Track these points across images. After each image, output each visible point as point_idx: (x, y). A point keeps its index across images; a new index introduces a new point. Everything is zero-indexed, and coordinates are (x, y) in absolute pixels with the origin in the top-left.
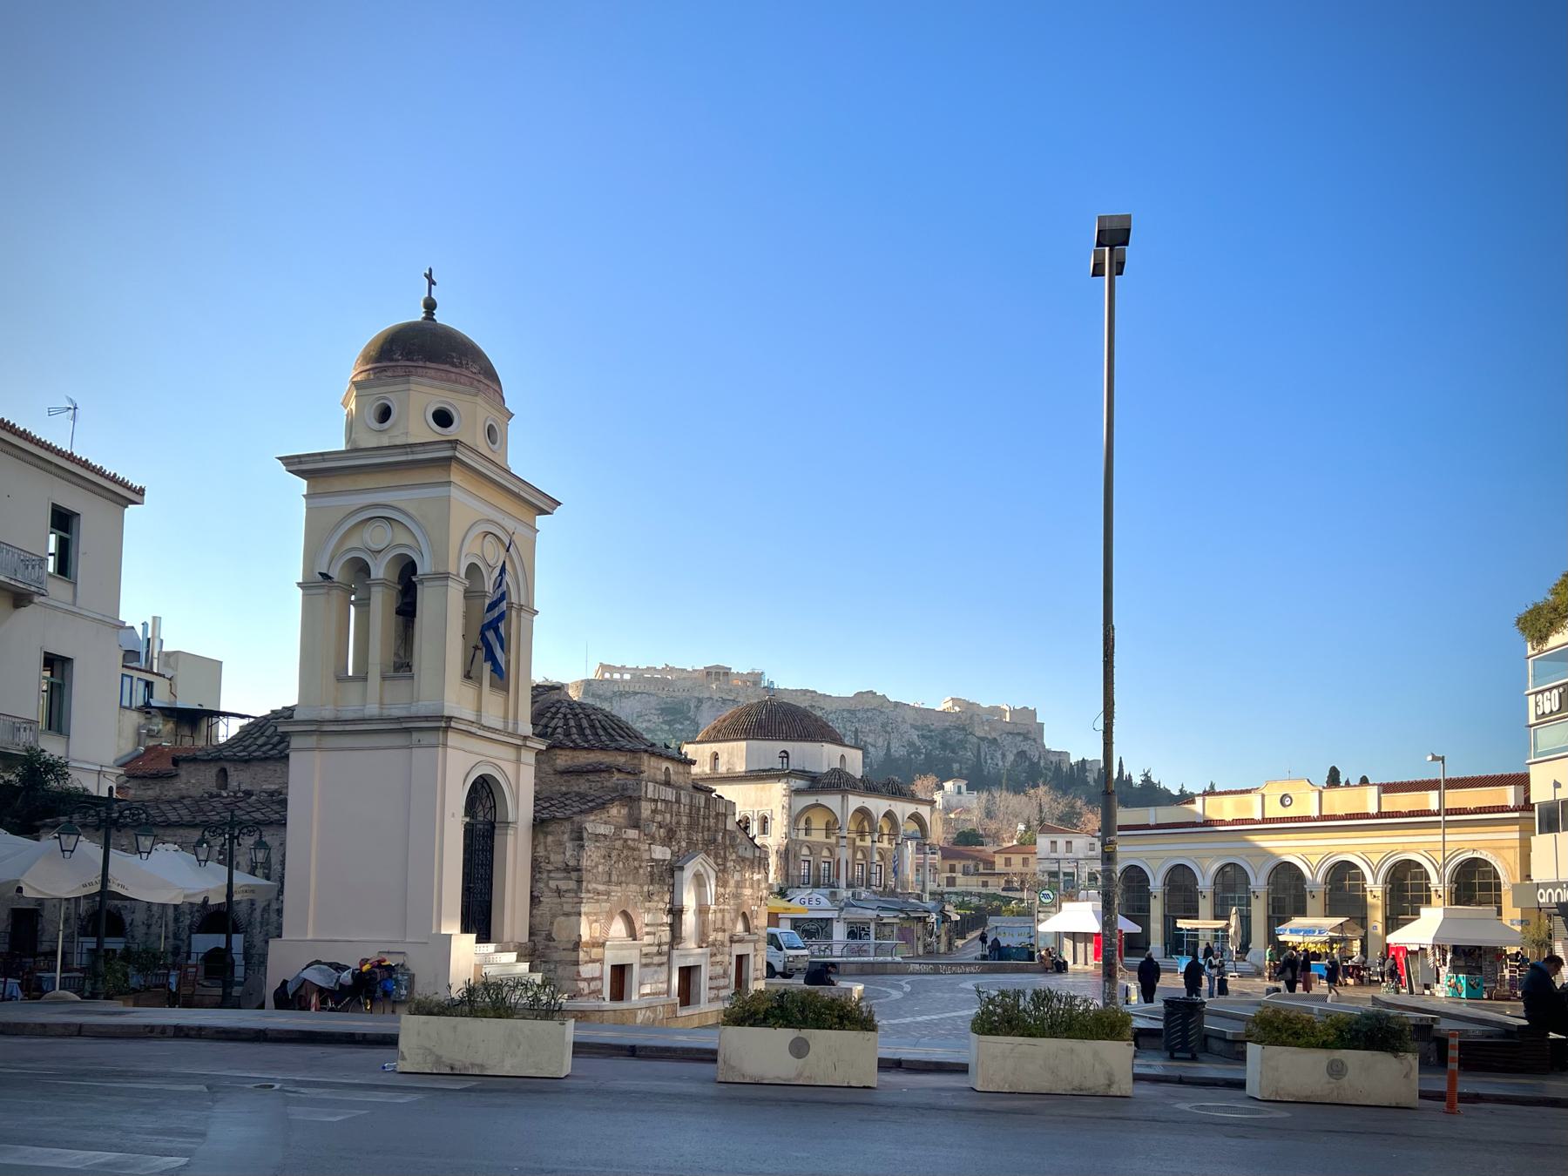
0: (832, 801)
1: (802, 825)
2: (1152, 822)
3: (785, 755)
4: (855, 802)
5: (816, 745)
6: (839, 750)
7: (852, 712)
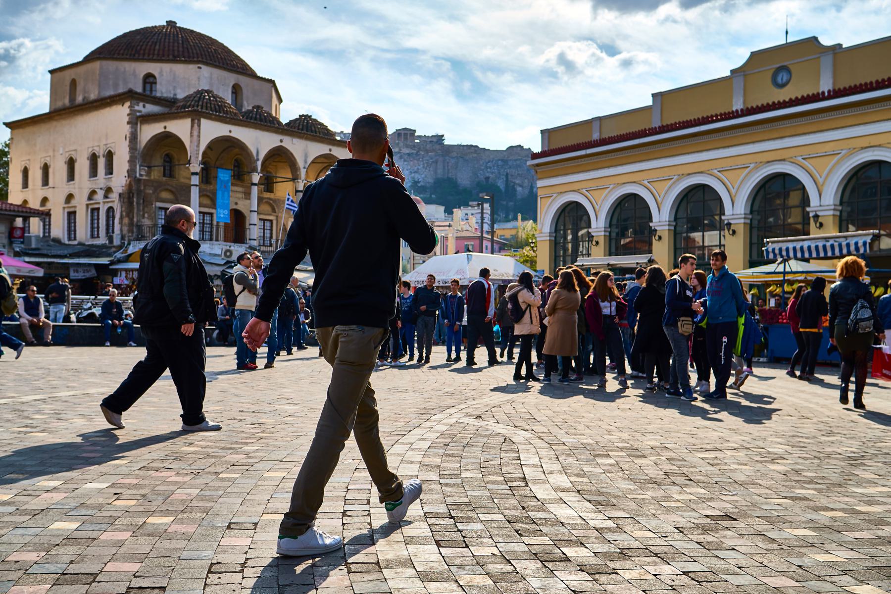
0: (180, 128)
1: (158, 161)
2: (596, 136)
3: (149, 79)
4: (213, 129)
5: (192, 68)
6: (232, 78)
7: (505, 161)
